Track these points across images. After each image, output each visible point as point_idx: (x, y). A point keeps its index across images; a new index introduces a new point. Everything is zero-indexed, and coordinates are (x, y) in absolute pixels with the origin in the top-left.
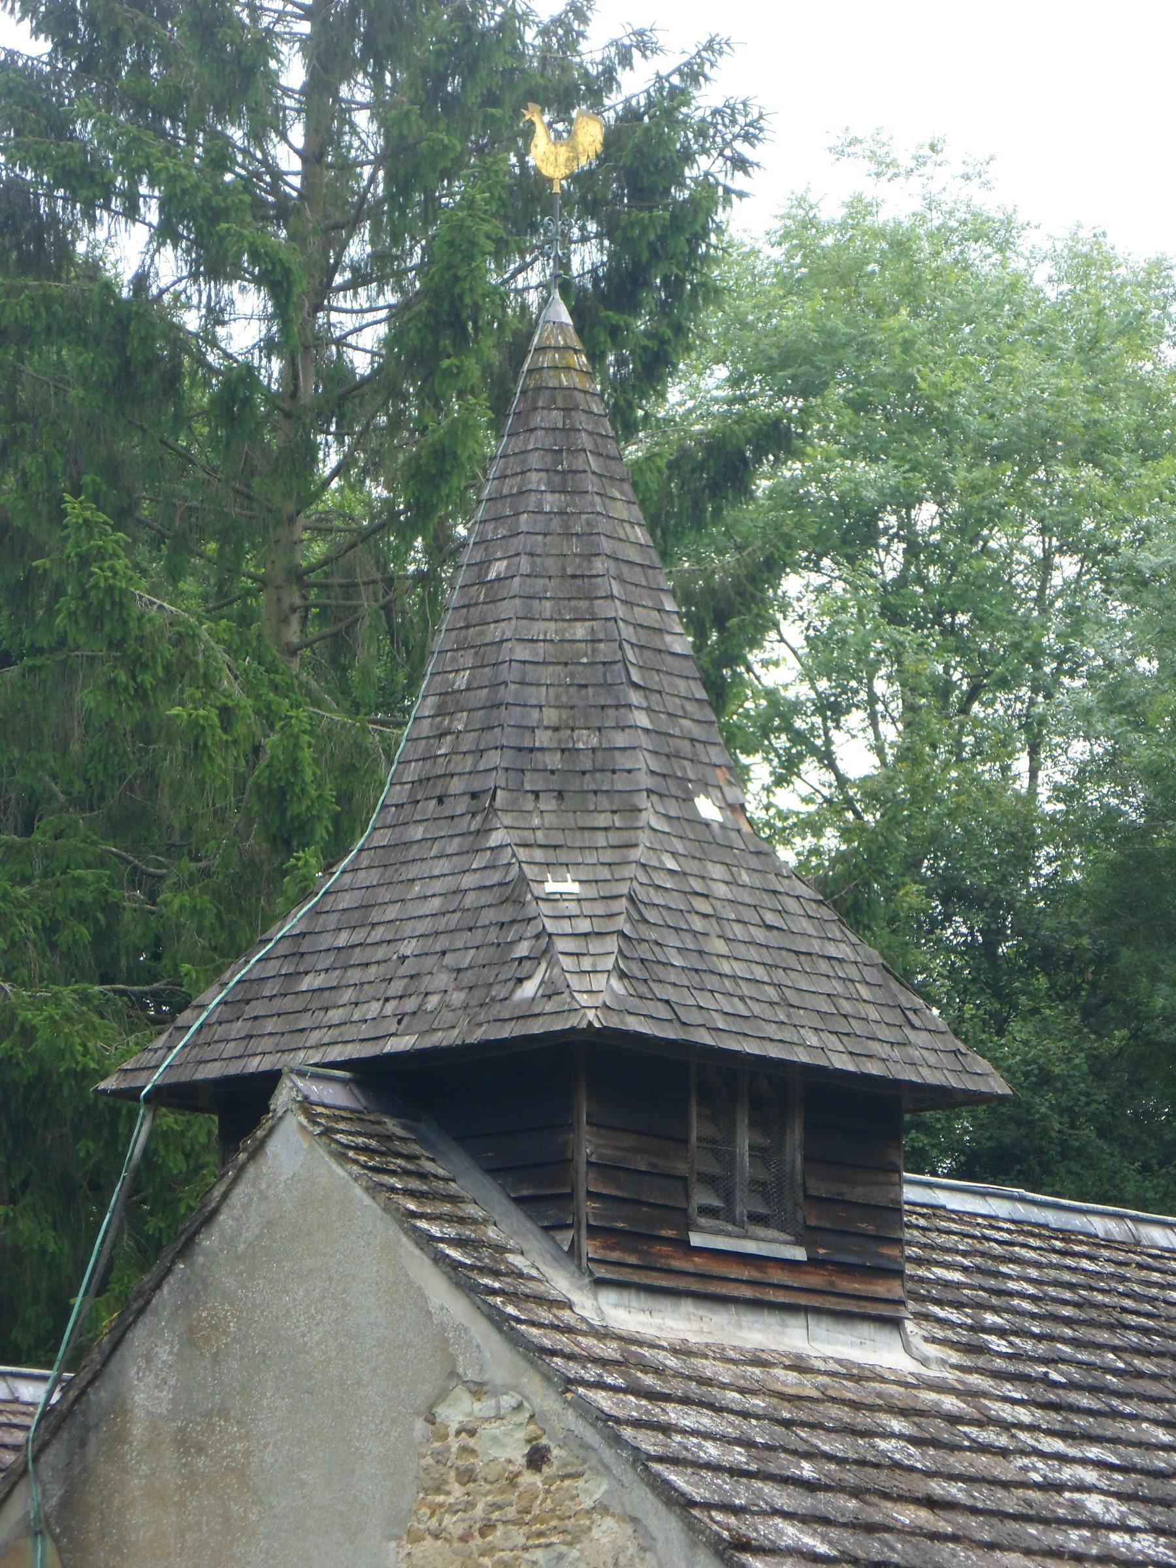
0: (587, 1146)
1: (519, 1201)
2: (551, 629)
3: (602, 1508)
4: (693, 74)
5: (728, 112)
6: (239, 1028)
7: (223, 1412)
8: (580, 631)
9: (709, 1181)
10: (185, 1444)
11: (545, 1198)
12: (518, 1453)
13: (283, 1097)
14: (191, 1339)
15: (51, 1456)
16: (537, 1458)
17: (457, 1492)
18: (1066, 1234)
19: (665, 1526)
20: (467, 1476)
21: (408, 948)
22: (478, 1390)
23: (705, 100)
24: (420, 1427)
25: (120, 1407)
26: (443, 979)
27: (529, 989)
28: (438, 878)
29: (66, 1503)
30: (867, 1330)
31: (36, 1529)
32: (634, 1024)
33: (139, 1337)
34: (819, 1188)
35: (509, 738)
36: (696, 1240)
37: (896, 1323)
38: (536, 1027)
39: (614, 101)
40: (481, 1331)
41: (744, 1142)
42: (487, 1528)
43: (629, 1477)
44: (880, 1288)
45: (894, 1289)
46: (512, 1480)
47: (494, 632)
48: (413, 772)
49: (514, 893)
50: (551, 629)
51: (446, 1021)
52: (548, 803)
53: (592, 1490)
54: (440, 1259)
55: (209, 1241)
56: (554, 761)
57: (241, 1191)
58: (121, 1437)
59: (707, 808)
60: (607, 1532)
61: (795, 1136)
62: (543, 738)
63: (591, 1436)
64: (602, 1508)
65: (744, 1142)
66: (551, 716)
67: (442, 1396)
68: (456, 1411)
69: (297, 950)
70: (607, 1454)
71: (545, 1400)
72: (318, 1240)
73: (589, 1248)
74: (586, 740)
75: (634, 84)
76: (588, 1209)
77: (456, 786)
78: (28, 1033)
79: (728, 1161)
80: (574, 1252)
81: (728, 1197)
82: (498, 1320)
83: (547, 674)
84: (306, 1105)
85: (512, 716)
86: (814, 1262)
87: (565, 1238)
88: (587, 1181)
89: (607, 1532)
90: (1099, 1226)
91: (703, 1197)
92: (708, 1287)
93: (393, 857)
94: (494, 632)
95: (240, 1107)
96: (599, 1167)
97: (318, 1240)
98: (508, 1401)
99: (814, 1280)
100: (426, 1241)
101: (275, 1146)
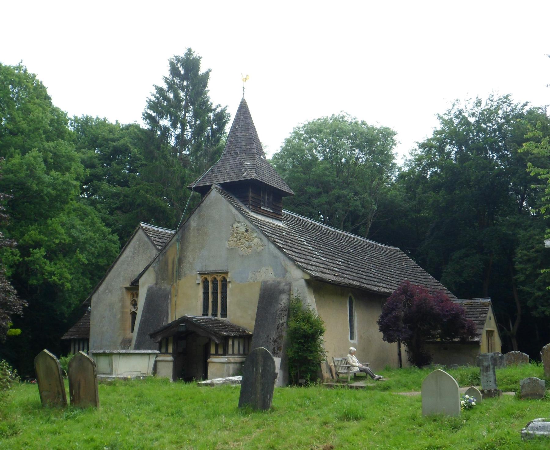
0: (251, 195)
1: (241, 201)
2: (244, 134)
3: (256, 237)
5: (228, 114)
6: (205, 180)
7: (204, 226)
8: (248, 134)
9: (263, 201)
10: (198, 230)
11: (245, 201)
12: (244, 230)
13: (213, 187)
14: (199, 217)
15: (180, 232)
16: (247, 231)
17: (235, 235)
19: (265, 239)
20: (237, 233)
21: (227, 170)
22: (239, 222)
23: (227, 112)
24: (231, 227)
25: (189, 225)
26: (232, 174)
27: (245, 174)
28: (230, 163)
29: (182, 238)
30: (278, 221)
31: (177, 241)
33: (192, 217)
35: (239, 146)
37: (281, 221)
38: (246, 179)
39: (217, 112)
40: (240, 215)
41: (266, 197)
42: (240, 239)
43: (260, 233)
46: (243, 234)
47: (237, 134)
48: (226, 151)
49: (241, 164)
50: (244, 134)
51: (233, 178)
52: (244, 154)
53: (255, 235)
54: (234, 206)
55: (202, 205)
56: (245, 149)
57: (207, 198)
58: (190, 229)
59: (262, 157)
60: (256, 240)
61: (272, 197)
62: (243, 147)
63: (255, 228)
64: (256, 237)
65: (266, 197)
66: (244, 144)
67: (234, 223)
68: (235, 225)
69: (212, 171)
70: (257, 230)
71: (248, 223)
72: (217, 204)
73: (251, 207)
74: (249, 147)
75: (219, 110)
77: (232, 152)
78: (155, 202)
80: (249, 208)
81: (264, 203)
82: (242, 214)
83: (244, 139)
84: (216, 188)
85: (240, 144)
86: (273, 212)
87: (248, 206)
88: (250, 199)
89: (256, 240)
91: (262, 203)
92: (263, 213)
93: (225, 160)
94: (237, 134)
95: (204, 190)
97: (217, 204)
98: (243, 224)
99: (273, 214)
100: (232, 204)
101: (211, 193)
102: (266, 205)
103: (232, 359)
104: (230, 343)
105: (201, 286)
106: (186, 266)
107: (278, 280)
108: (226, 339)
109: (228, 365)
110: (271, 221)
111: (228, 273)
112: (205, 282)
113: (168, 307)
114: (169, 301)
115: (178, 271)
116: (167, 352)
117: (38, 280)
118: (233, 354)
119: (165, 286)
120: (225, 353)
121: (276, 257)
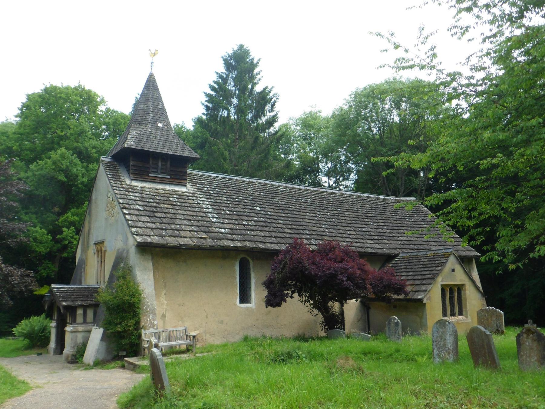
0: (131, 163)
4: (271, 90)
18: (229, 179)
22: (110, 192)
30: (180, 186)
32: (133, 147)
34: (173, 169)
36: (150, 175)
37: (185, 186)
41: (160, 164)
44: (183, 182)
45: (185, 181)
61: (169, 163)
65: (160, 164)
66: (141, 115)
73: (131, 176)
76: (131, 171)
79: (158, 165)
86: (171, 178)
88: (131, 167)
90: (236, 178)
96: (133, 166)
99: (171, 180)
102: (159, 172)
103: (81, 328)
104: (80, 312)
105: (96, 255)
106: (91, 236)
107: (124, 247)
108: (72, 310)
109: (74, 334)
110: (168, 187)
111: (102, 242)
112: (98, 251)
113: (81, 276)
114: (83, 270)
115: (88, 242)
116: (54, 320)
117: (69, 253)
118: (85, 322)
119: (84, 257)
120: (74, 321)
121: (123, 224)
